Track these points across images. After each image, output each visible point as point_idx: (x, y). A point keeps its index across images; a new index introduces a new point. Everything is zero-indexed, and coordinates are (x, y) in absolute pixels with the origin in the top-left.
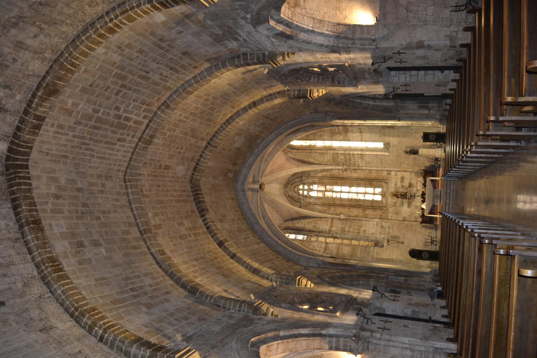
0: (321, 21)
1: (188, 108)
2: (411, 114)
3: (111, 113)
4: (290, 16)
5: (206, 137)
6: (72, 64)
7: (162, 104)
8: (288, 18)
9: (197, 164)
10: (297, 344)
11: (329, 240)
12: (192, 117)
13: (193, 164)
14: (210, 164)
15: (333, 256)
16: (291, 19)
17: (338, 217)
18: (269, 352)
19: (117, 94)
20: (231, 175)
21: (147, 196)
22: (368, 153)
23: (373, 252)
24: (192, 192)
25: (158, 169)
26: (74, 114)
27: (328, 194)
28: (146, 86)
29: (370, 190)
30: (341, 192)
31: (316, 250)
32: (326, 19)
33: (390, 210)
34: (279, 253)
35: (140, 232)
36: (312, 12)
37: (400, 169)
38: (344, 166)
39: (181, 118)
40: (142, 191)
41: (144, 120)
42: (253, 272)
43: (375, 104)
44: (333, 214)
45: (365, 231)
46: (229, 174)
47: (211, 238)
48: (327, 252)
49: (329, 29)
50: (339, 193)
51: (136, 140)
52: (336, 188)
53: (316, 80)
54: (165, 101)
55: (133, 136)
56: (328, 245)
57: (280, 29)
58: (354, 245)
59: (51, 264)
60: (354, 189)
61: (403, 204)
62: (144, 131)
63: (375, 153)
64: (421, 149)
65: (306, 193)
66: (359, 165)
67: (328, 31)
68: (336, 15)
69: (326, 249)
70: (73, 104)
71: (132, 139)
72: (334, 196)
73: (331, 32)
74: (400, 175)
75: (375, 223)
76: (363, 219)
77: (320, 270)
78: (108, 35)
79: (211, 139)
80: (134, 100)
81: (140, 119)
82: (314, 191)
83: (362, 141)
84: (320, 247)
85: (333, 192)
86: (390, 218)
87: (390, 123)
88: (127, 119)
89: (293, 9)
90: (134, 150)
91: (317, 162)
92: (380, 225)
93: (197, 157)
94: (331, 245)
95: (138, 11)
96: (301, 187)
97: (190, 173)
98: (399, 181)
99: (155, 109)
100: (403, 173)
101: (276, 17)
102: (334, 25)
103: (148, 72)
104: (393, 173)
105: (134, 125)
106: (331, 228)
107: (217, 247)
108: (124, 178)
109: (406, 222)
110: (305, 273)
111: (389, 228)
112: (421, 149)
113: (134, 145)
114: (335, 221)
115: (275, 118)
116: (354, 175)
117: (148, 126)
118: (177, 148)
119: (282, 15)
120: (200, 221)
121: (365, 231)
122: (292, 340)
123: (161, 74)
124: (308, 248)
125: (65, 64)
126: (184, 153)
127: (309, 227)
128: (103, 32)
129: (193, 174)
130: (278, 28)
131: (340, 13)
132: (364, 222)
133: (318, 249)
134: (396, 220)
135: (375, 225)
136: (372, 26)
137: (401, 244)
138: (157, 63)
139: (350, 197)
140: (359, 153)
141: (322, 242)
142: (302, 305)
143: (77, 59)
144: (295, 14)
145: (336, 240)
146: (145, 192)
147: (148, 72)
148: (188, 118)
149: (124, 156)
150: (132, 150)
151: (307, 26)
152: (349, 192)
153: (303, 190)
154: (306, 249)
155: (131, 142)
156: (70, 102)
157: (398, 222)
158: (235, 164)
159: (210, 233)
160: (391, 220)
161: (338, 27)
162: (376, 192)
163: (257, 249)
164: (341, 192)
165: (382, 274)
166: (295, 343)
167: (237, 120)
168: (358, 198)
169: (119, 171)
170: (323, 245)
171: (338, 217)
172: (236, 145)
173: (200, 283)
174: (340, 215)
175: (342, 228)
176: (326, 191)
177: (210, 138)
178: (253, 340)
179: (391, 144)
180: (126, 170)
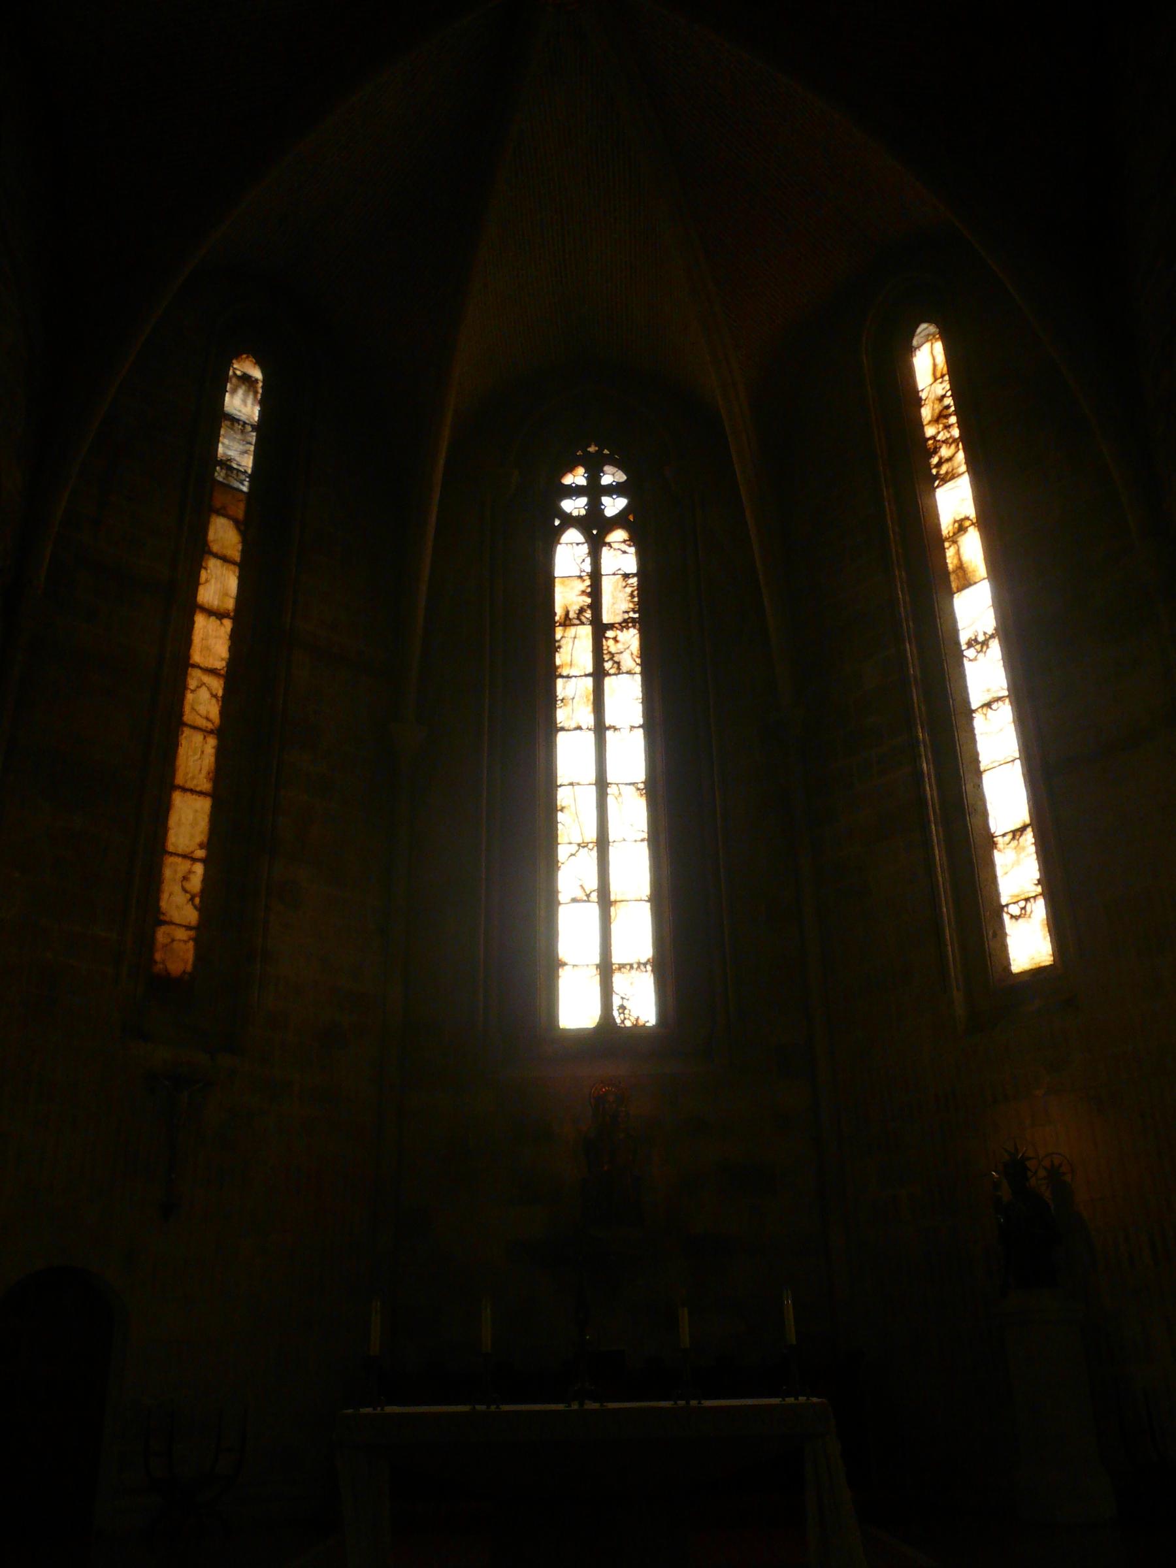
27: (574, 650)
29: (636, 934)
30: (600, 729)
50: (589, 720)
52: (626, 696)
60: (631, 816)
63: (946, 910)
72: (562, 688)
85: (599, 675)
140: (930, 791)
145: (217, 685)
152: (602, 784)
153: (594, 491)
162: (619, 981)
164: (600, 729)
168: (563, 852)
176: (600, 630)
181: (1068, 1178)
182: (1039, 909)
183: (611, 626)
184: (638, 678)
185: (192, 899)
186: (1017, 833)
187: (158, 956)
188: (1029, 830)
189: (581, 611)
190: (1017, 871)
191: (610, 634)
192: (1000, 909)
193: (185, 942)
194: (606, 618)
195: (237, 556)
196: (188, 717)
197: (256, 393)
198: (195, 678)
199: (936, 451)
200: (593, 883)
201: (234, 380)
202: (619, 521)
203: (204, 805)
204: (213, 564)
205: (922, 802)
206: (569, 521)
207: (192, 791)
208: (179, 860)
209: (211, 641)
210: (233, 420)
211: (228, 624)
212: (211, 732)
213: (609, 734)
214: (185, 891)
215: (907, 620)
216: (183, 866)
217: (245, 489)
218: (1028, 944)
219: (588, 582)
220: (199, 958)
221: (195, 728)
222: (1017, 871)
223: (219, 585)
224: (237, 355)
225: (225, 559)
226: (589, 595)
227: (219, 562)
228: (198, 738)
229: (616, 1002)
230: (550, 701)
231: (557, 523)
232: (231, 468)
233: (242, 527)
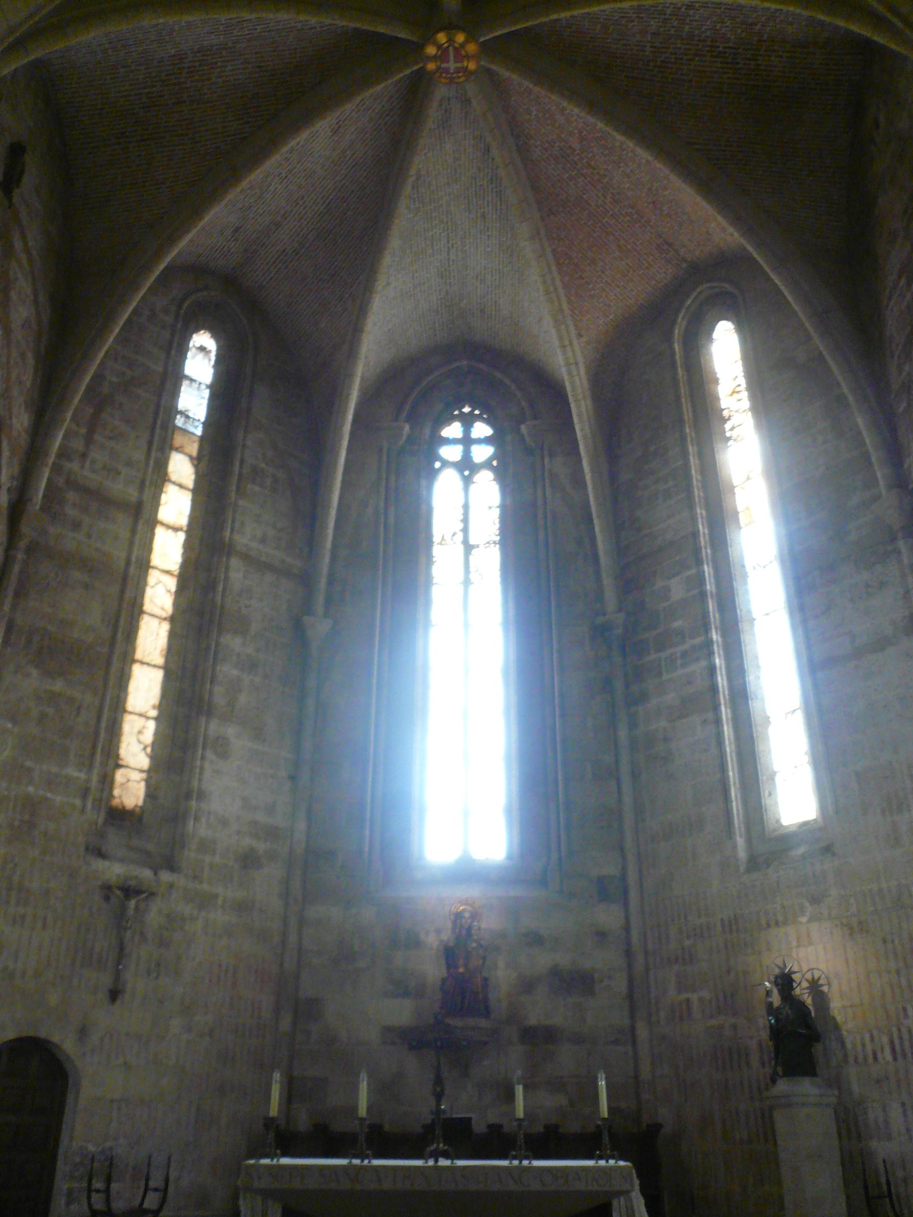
22: (727, 730)
23: (50, 782)
37: (640, 959)
38: (622, 615)
45: (222, 748)
48: (71, 496)
61: (406, 994)
63: (732, 774)
65: (451, 453)
66: (643, 697)
82: (466, 489)
92: (261, 847)
94: (125, 534)
96: (482, 430)
98: (563, 959)
100: (620, 984)
106: (246, 557)
109: (286, 1024)
111: (242, 907)
121: (222, 748)
135: (261, 817)
137: (106, 980)
140: (722, 681)
153: (467, 441)
170: (122, 488)
176: (468, 548)
181: (825, 989)
185: (145, 748)
187: (116, 792)
188: (799, 711)
189: (454, 534)
193: (138, 782)
195: (191, 485)
197: (210, 360)
198: (153, 577)
199: (729, 419)
201: (194, 350)
202: (487, 465)
203: (158, 676)
205: (714, 689)
206: (445, 464)
207: (148, 664)
208: (136, 718)
209: (168, 550)
211: (182, 536)
212: (165, 619)
214: (139, 742)
215: (706, 548)
216: (139, 722)
217: (199, 431)
219: (462, 511)
220: (151, 795)
221: (152, 615)
223: (176, 505)
224: (197, 330)
225: (181, 486)
226: (462, 521)
227: (177, 488)
228: (155, 622)
231: (437, 465)
232: (187, 417)
233: (197, 461)
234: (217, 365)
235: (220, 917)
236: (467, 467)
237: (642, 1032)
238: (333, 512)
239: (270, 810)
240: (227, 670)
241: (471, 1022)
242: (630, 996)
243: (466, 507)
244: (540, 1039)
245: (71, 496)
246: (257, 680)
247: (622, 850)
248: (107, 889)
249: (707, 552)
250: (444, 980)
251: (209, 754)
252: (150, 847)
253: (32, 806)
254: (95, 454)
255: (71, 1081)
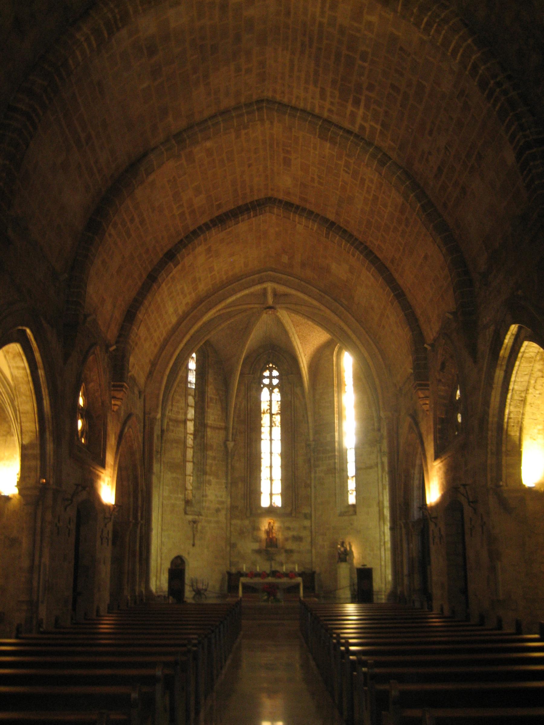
0: (524, 401)
1: (384, 193)
2: (402, 546)
3: (363, 78)
4: (526, 355)
5: (342, 220)
6: (429, 25)
7: (385, 154)
8: (524, 352)
9: (298, 207)
10: (26, 396)
11: (190, 426)
12: (371, 198)
13: (296, 201)
14: (300, 228)
15: (165, 433)
16: (522, 357)
17: (230, 438)
18: (11, 356)
19: (393, 87)
20: (285, 259)
21: (238, 137)
24: (252, 203)
25: (283, 150)
26: (356, 25)
27: (265, 420)
28: (410, 130)
29: (278, 487)
31: (172, 405)
32: (528, 409)
33: (247, 522)
34: (162, 348)
35: (180, 134)
36: (538, 387)
37: (314, 534)
38: (314, 443)
39: (367, 182)
40: (245, 128)
41: (357, 126)
42: (128, 311)
43: (415, 489)
44: (233, 429)
45: (209, 483)
46: (287, 257)
47: (180, 238)
48: (171, 423)
49: (512, 416)
51: (326, 114)
52: (277, 431)
53: (442, 394)
54: (390, 159)
55: (330, 111)
56: (182, 425)
57: (506, 341)
58: (185, 466)
59: (118, 17)
62: (341, 128)
64: (349, 566)
65: (266, 381)
67: (509, 414)
68: (536, 424)
69: (177, 421)
70: (370, 23)
71: (326, 110)
73: (509, 418)
74: (304, 534)
75: (223, 499)
76: (229, 478)
77: (141, 415)
78: (477, 79)
79: (340, 228)
80: (386, 113)
81: (359, 121)
82: (271, 395)
83: (357, 469)
84: (178, 412)
85: (271, 426)
86: (234, 522)
87: (387, 513)
88: (357, 102)
89: (538, 358)
90: (309, 113)
91: (317, 397)
92: (220, 507)
93: (308, 206)
94: (183, 430)
95: (513, 128)
96: (275, 373)
97: (281, 196)
98: (295, 533)
99: (376, 143)
100: (309, 539)
101: (522, 336)
102: (518, 421)
103: (431, 133)
104: (307, 523)
105: (348, 112)
106: (211, 427)
107: (166, 250)
108: (262, 101)
109: (228, 548)
110: (134, 393)
111: (217, 522)
112: (349, 566)
113: (317, 111)
114: (222, 434)
115: (384, 327)
116: (300, 461)
117: (349, 132)
118: (319, 177)
119: (526, 343)
120: (205, 219)
121: (209, 483)
122: (32, 388)
123: (430, 153)
124: (175, 391)
125: (429, 14)
126: (313, 187)
127: (211, 391)
128: (480, 72)
129: (280, 201)
130: (508, 337)
131: (539, 430)
132: (224, 481)
133: (175, 409)
134: (231, 532)
135: (220, 499)
136: (520, 480)
137: (191, 542)
138: (446, 148)
139: (263, 455)
141: (186, 414)
142: (84, 395)
143: (438, 31)
144: (530, 362)
145: (192, 437)
146: (243, 132)
147: (431, 133)
148: (368, 192)
149: (298, 97)
150: (309, 108)
151: (515, 381)
154: (174, 389)
155: (322, 107)
156: (373, 19)
157: (228, 535)
158: (303, 265)
159: (186, 237)
160: (231, 524)
161: (517, 429)
163: (166, 313)
165: (142, 516)
166: (28, 393)
167: (373, 268)
169: (275, 91)
170: (181, 417)
171: (230, 438)
172: (334, 266)
173: (107, 235)
174: (234, 440)
175: (211, 446)
176: (271, 415)
177: (342, 225)
178: (28, 331)
179: (354, 517)
180: (276, 102)
182: (354, 493)
183: (274, 414)
184: (280, 428)
186: (352, 477)
189: (267, 410)
190: (352, 484)
191: (274, 416)
192: (348, 491)
194: (273, 412)
195: (193, 405)
196: (188, 445)
200: (269, 476)
204: (190, 408)
206: (265, 385)
210: (190, 370)
211: (193, 422)
213: (273, 441)
217: (194, 387)
218: (352, 499)
219: (269, 403)
220: (194, 496)
221: (189, 447)
222: (352, 484)
225: (192, 406)
229: (273, 501)
230: (260, 433)
231: (262, 386)
233: (194, 397)
234: (196, 363)
235: (213, 525)
236: (271, 387)
237: (314, 551)
238: (233, 409)
239: (221, 497)
240: (209, 461)
241: (273, 549)
242: (311, 542)
243: (271, 401)
244: (289, 552)
245: (171, 423)
246: (216, 462)
247: (311, 507)
248: (189, 522)
249: (337, 428)
250: (266, 539)
251: (207, 485)
252: (195, 509)
253: (173, 505)
254: (174, 409)
255: (186, 564)
